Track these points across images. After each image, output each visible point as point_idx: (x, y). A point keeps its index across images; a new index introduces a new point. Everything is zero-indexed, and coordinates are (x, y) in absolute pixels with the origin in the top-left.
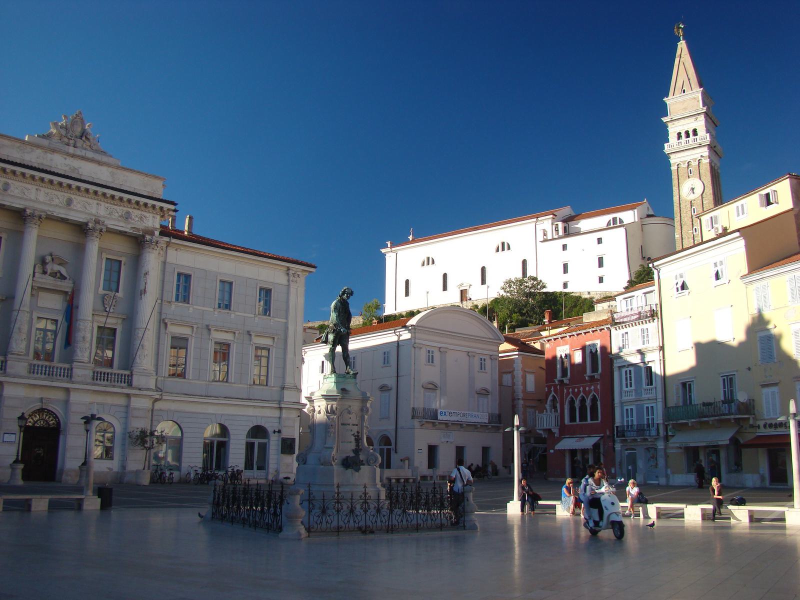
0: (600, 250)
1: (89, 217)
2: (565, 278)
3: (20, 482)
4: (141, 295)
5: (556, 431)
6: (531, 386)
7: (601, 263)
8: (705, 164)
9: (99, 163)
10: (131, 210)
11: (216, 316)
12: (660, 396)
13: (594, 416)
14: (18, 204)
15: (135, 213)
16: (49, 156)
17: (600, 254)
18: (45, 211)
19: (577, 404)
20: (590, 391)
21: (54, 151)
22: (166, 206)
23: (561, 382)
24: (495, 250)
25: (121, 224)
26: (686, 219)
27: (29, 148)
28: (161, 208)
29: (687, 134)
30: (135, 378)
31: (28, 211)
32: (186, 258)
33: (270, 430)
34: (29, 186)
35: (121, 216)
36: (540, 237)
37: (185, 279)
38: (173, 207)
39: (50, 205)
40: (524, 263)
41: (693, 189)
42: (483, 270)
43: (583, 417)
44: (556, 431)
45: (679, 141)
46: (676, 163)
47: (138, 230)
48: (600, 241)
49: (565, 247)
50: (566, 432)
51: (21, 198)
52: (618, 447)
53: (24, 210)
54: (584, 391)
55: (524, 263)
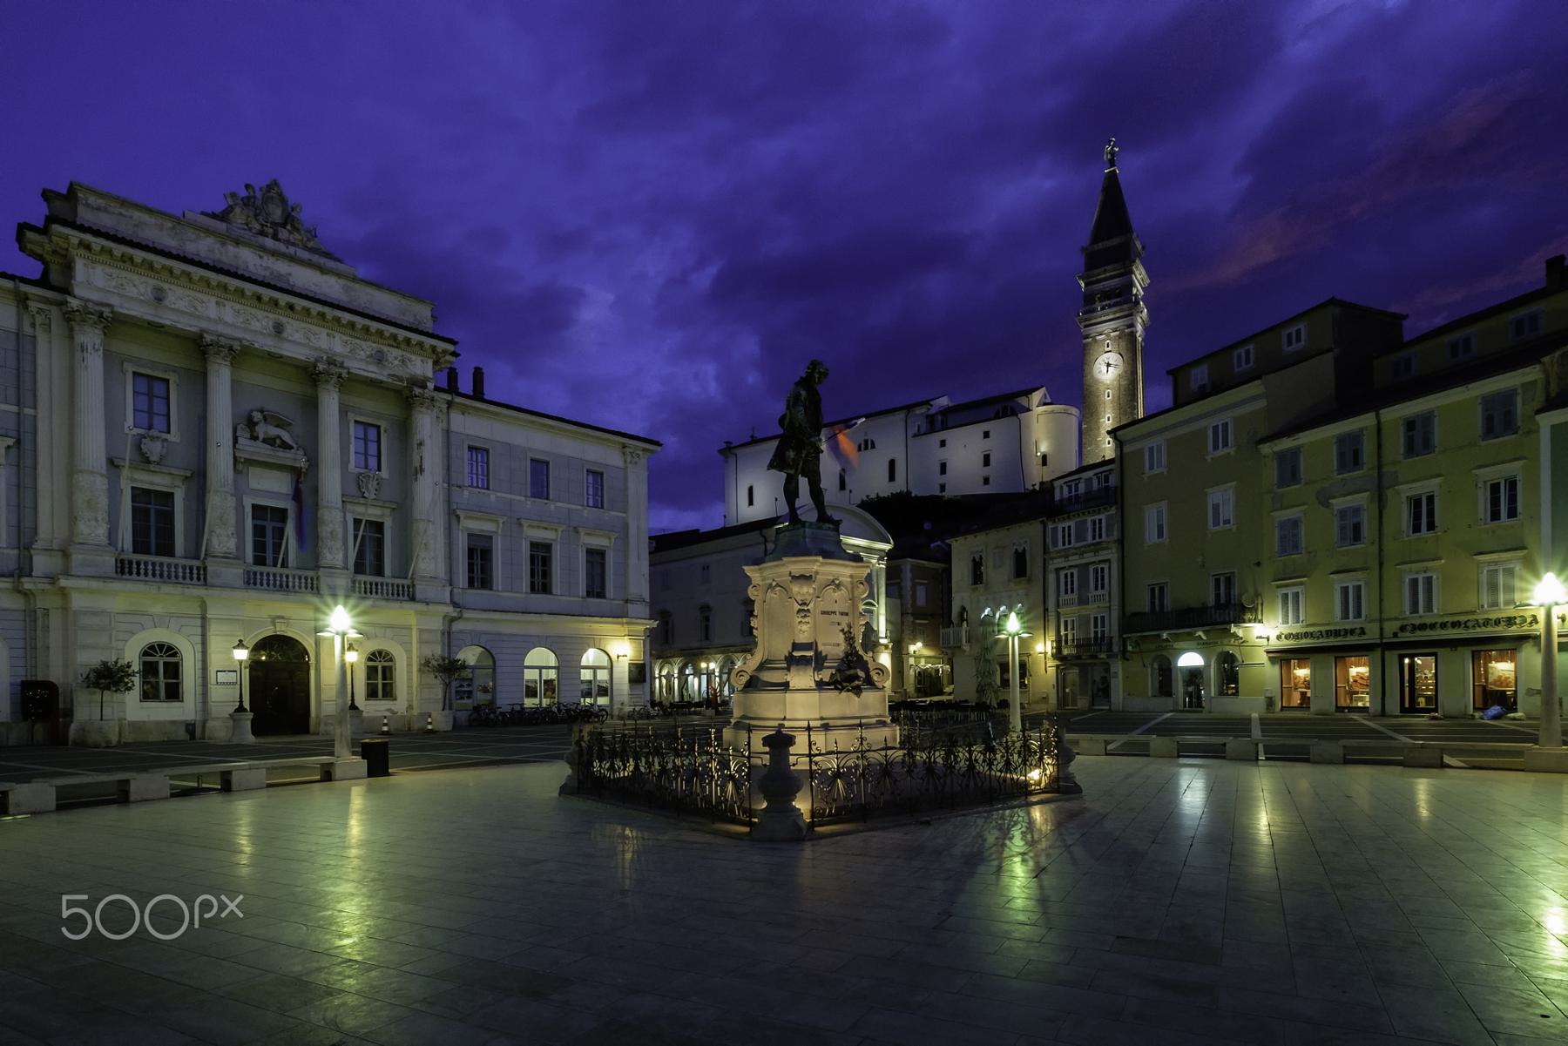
1: (316, 354)
3: (250, 739)
10: (385, 349)
11: (524, 502)
15: (393, 354)
18: (240, 340)
22: (441, 345)
25: (373, 368)
28: (434, 348)
31: (208, 338)
32: (472, 425)
34: (205, 298)
35: (370, 356)
38: (451, 348)
39: (245, 330)
47: (400, 379)
51: (191, 315)
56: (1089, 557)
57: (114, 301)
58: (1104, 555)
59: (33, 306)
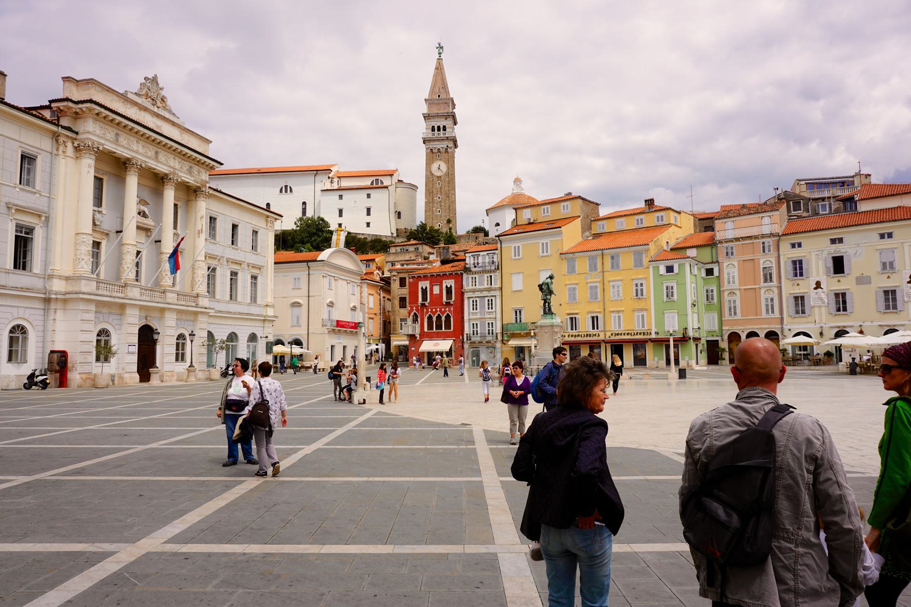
2: (340, 220)
4: (199, 233)
5: (418, 336)
6: (371, 306)
7: (369, 211)
9: (174, 124)
12: (499, 316)
13: (448, 326)
14: (126, 154)
15: (196, 168)
16: (143, 113)
17: (368, 205)
19: (434, 319)
20: (445, 311)
21: (146, 109)
23: (423, 305)
27: (129, 106)
29: (439, 128)
30: (200, 299)
33: (259, 336)
36: (320, 186)
37: (212, 220)
39: (147, 157)
40: (304, 203)
43: (439, 327)
44: (418, 336)
48: (369, 196)
49: (341, 197)
50: (424, 336)
51: (128, 149)
52: (466, 346)
53: (128, 159)
54: (441, 311)
55: (304, 203)
56: (485, 294)
57: (102, 141)
58: (492, 293)
59: (61, 139)
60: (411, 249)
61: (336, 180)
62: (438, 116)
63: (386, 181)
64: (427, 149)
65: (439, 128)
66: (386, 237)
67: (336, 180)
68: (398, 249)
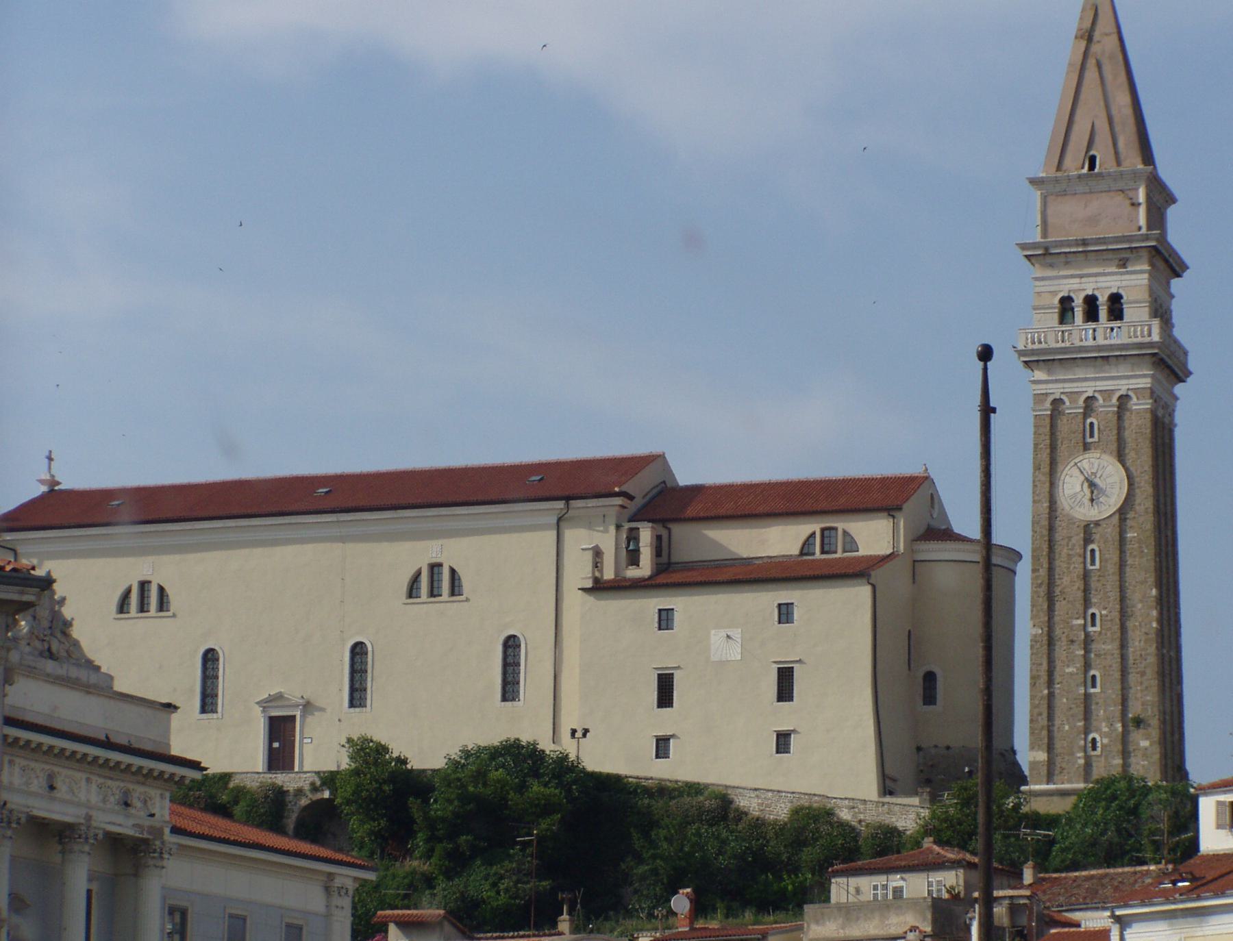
0: (783, 645)
8: (1138, 412)
9: (88, 689)
10: (131, 786)
15: (138, 791)
24: (404, 589)
25: (120, 819)
26: (1066, 580)
29: (1091, 301)
36: (578, 572)
40: (511, 644)
41: (1092, 485)
42: (358, 651)
45: (1064, 328)
46: (1046, 394)
48: (785, 613)
49: (665, 619)
55: (511, 644)
60: (917, 885)
61: (646, 535)
62: (1086, 252)
63: (873, 536)
64: (1039, 398)
65: (1091, 301)
66: (853, 803)
67: (646, 535)
68: (867, 886)
